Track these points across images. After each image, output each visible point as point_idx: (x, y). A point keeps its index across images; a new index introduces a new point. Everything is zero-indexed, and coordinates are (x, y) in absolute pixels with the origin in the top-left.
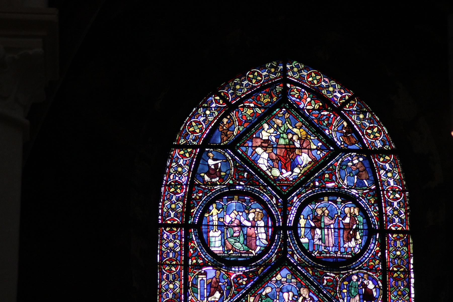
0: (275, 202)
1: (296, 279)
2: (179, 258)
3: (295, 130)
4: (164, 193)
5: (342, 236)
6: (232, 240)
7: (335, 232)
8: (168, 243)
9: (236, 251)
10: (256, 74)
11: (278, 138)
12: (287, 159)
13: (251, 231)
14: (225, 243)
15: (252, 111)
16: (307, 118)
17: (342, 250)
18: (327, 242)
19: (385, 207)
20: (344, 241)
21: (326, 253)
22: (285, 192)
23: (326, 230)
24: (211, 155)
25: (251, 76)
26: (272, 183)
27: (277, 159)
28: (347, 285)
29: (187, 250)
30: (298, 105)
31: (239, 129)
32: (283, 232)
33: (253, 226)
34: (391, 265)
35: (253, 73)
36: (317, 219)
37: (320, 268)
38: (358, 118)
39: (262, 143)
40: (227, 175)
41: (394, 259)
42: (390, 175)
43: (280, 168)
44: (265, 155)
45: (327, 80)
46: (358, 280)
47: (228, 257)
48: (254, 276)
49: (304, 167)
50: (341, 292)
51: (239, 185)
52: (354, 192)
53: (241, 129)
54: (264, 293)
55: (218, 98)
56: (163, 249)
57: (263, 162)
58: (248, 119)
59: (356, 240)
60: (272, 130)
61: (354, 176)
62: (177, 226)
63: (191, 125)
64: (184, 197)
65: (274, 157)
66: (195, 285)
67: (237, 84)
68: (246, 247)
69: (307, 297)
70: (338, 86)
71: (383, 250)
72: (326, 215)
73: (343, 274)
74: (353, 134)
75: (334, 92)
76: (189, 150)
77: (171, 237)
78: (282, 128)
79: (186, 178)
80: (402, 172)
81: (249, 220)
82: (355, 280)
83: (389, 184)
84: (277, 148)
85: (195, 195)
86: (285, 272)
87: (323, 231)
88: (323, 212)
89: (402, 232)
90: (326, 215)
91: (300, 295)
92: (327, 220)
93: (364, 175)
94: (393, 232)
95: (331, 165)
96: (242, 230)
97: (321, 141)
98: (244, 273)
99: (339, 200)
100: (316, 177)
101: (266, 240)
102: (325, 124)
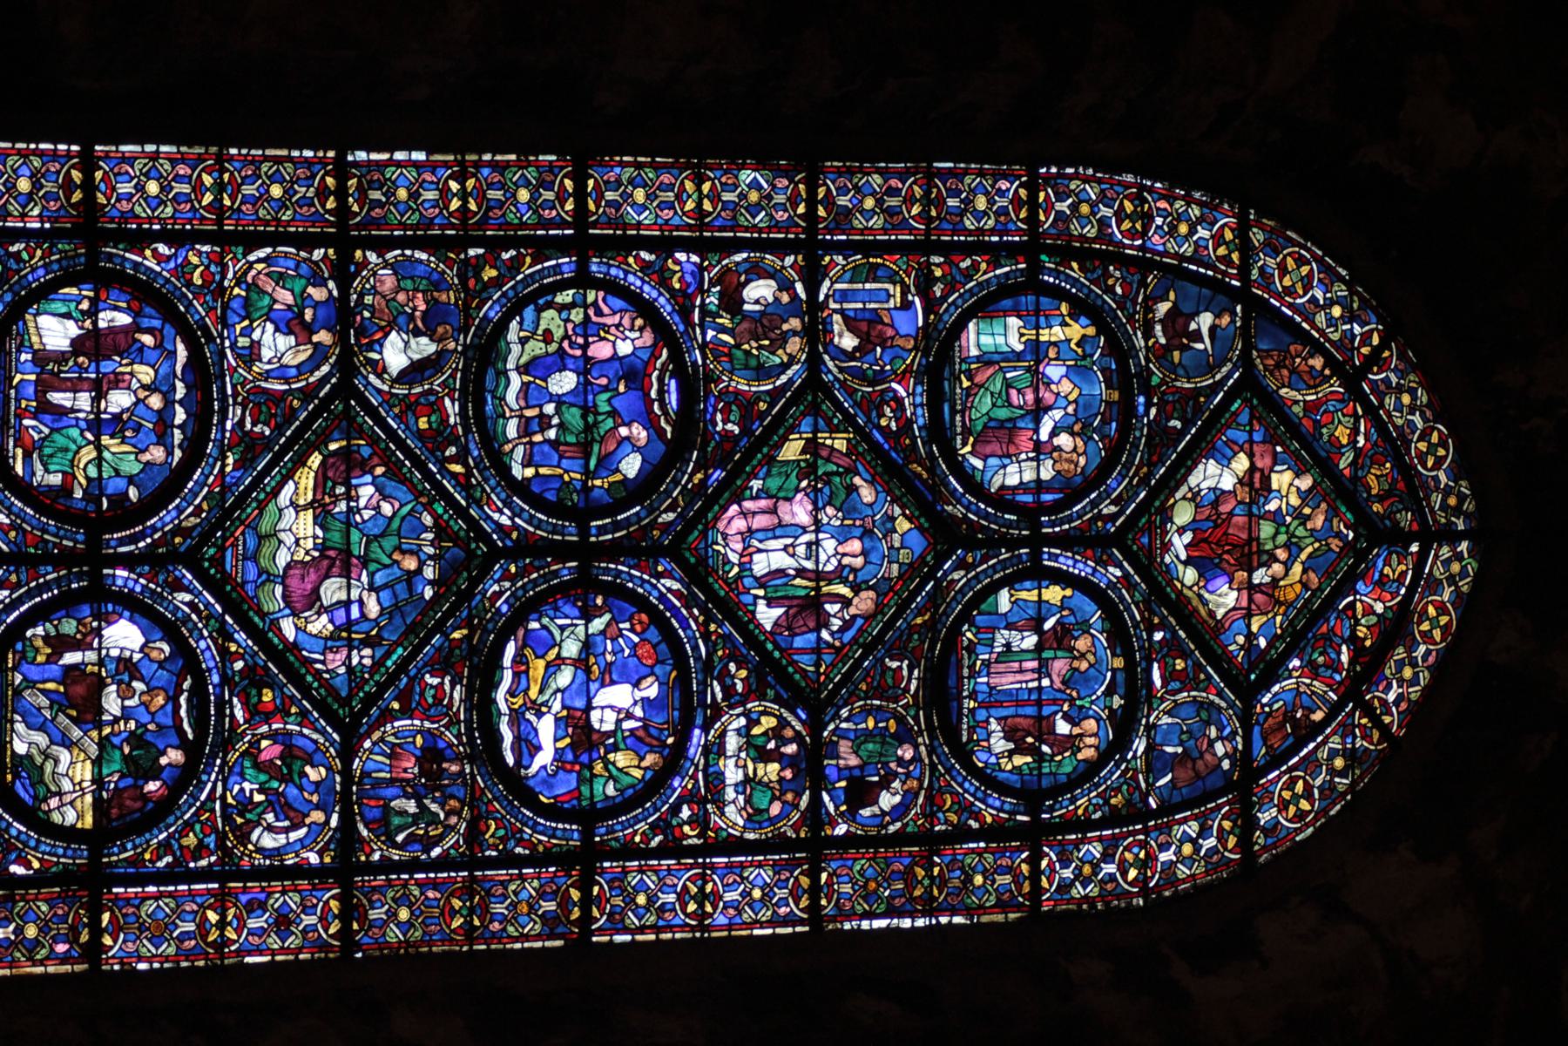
0: (1105, 511)
1: (900, 577)
2: (946, 226)
3: (1297, 569)
4: (1120, 183)
5: (1021, 711)
6: (997, 385)
7: (1030, 690)
8: (986, 193)
9: (968, 396)
10: (1441, 452)
11: (1276, 517)
12: (1225, 547)
13: (1024, 441)
14: (989, 363)
15: (1345, 441)
16: (1330, 603)
17: (981, 715)
18: (1001, 667)
19: (1100, 839)
20: (1006, 718)
21: (972, 667)
22: (1134, 540)
23: (1035, 664)
24: (1226, 320)
25: (1435, 438)
26: (1157, 503)
27: (1219, 515)
28: (886, 728)
29: (967, 249)
30: (1363, 576)
31: (1296, 402)
32: (1025, 534)
33: (1038, 447)
34: (947, 859)
35: (1443, 443)
36: (1061, 639)
37: (932, 648)
38: (1333, 754)
39: (1262, 470)
40: (1173, 368)
41: (962, 869)
42: (1188, 849)
43: (1193, 526)
44: (1228, 483)
45: (1431, 659)
46: (900, 761)
47: (952, 373)
48: (903, 450)
49: (1200, 596)
50: (867, 711)
51: (1148, 405)
52: (1140, 745)
53: (1296, 409)
54: (857, 480)
55: (1376, 340)
56: (968, 180)
57: (1213, 476)
58: (1324, 431)
59: (1011, 753)
60: (1294, 501)
61: (1181, 743)
62: (1032, 220)
63: (1301, 261)
64: (1110, 239)
65: (1225, 508)
66: (872, 273)
67: (1414, 398)
68: (979, 428)
69: (853, 610)
70: (1414, 692)
71: (985, 833)
72: (1076, 664)
73: (916, 718)
74: (1291, 740)
75: (1401, 682)
76: (1235, 257)
77: (1001, 202)
78: (1300, 532)
79: (1161, 248)
80: (1195, 887)
81: (1053, 434)
82: (900, 752)
83: (1163, 847)
84: (1250, 515)
85: (1118, 274)
86: (918, 542)
87: (1030, 656)
88: (1083, 656)
89: (1037, 890)
90: (1076, 664)
91: (856, 589)
92: (1060, 666)
93: (1185, 774)
94: (1034, 861)
95: (1209, 677)
96: (1028, 412)
97: (1270, 645)
98: (910, 422)
99: (1117, 702)
100: (1175, 633)
101: (1003, 487)
102: (1315, 655)
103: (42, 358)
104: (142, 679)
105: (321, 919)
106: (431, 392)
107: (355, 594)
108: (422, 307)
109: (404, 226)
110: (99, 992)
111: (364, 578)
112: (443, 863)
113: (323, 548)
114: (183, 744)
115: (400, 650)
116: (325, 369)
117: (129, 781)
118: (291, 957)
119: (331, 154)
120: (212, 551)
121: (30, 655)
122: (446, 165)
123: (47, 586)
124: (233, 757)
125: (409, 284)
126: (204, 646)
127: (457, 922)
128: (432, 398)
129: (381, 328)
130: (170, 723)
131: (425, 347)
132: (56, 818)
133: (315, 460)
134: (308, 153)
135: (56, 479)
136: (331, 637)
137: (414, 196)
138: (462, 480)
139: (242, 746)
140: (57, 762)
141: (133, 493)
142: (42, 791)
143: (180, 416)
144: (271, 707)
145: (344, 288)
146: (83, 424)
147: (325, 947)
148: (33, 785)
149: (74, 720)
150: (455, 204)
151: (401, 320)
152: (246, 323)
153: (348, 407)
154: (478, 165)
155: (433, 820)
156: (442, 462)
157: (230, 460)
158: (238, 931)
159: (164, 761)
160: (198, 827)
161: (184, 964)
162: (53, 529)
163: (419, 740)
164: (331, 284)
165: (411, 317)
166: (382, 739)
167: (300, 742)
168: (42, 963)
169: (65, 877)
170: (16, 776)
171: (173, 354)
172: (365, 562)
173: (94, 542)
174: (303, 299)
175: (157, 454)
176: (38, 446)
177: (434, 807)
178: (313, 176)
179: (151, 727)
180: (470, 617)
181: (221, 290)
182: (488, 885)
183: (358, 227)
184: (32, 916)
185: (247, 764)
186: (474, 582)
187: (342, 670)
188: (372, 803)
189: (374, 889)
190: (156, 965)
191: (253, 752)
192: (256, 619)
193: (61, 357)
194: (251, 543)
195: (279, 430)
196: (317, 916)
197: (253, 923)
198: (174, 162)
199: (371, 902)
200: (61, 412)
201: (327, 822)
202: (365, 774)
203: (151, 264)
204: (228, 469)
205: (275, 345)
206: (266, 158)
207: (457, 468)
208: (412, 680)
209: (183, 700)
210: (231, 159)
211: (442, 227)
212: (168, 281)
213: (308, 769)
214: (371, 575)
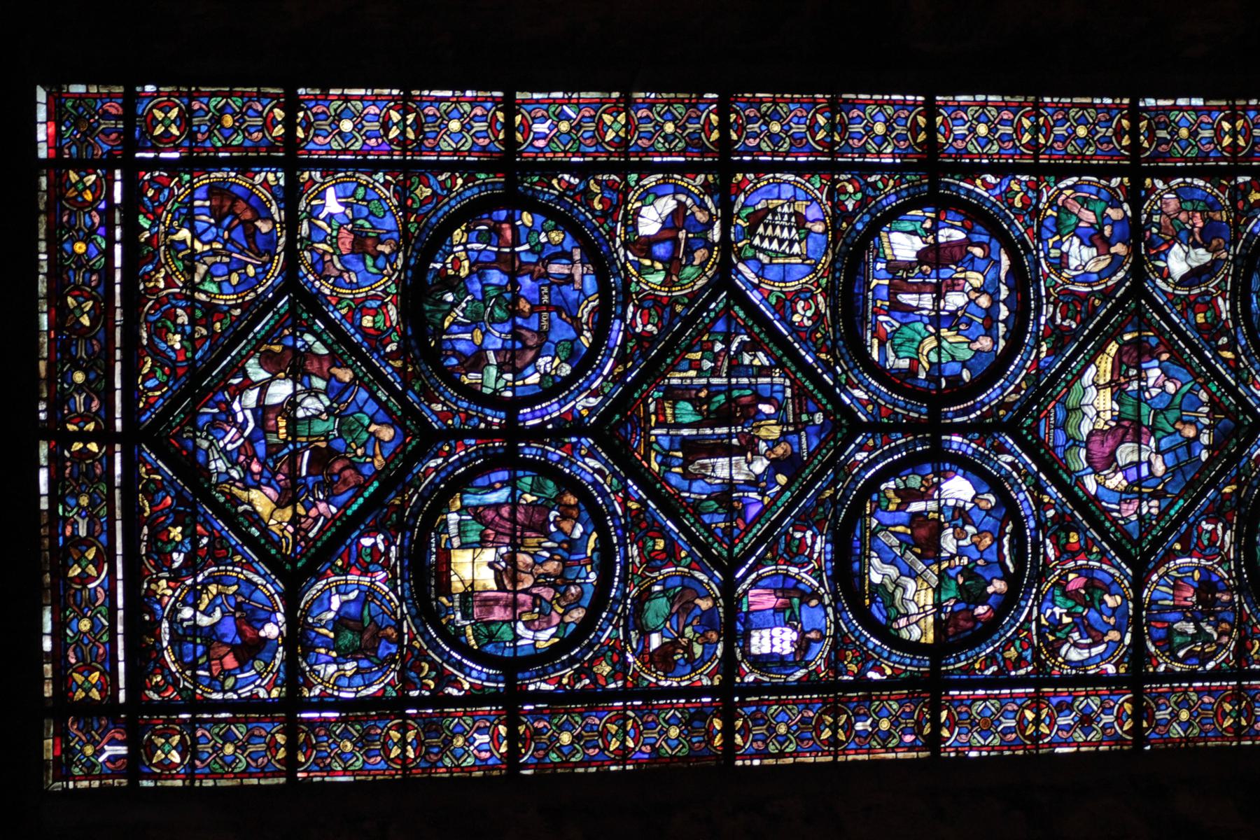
103: (894, 267)
104: (973, 524)
105: (1117, 718)
106: (1207, 293)
107: (1144, 456)
108: (1200, 224)
109: (1184, 159)
110: (938, 775)
111: (1152, 443)
112: (1216, 674)
113: (1119, 419)
114: (1006, 576)
115: (1181, 502)
116: (1121, 274)
117: (962, 606)
118: (1093, 749)
119: (1126, 101)
120: (1029, 421)
121: (884, 504)
122: (1220, 109)
123: (898, 449)
124: (1046, 587)
125: (1189, 205)
126: (1023, 497)
127: (1228, 723)
128: (1208, 298)
129: (1166, 242)
130: (995, 558)
131: (1202, 256)
132: (904, 634)
133: (1113, 348)
134: (1108, 101)
135: (904, 364)
136: (1126, 491)
137: (1193, 134)
138: (1232, 364)
139: (1053, 578)
140: (905, 590)
141: (966, 375)
142: (893, 613)
143: (1004, 312)
144: (1077, 547)
145: (1136, 209)
146: (926, 320)
147: (1119, 740)
148: (886, 608)
149: (919, 557)
150: (1227, 141)
151: (1183, 235)
152: (1057, 238)
153: (1139, 305)
154: (1246, 108)
155: (1208, 639)
156: (1216, 350)
157: (1044, 348)
158: (1050, 726)
159: (990, 590)
160: (1018, 643)
161: (1007, 753)
162: (902, 404)
163: (1197, 575)
164: (1126, 206)
165: (1191, 233)
166: (1166, 574)
167: (1100, 575)
168: (893, 750)
169: (912, 682)
170: (873, 601)
171: (999, 262)
172: (1153, 430)
173: (935, 414)
174: (1103, 218)
175: (985, 343)
176: (891, 336)
177: (1209, 629)
178: (1112, 119)
179: (980, 562)
180: (1239, 475)
181: (1037, 212)
182: (1252, 693)
183: (1148, 160)
184: (885, 713)
185: (1057, 592)
186: (1242, 447)
187: (1134, 518)
188: (1159, 625)
189: (1160, 695)
190: (984, 753)
191: (1062, 583)
192: (1065, 476)
193: (909, 266)
194: (1061, 415)
195: (1083, 324)
196: (1114, 717)
197: (1062, 721)
198: (999, 108)
199: (1158, 705)
200: (908, 309)
201: (1122, 640)
202: (1153, 602)
203: (981, 191)
204: (1043, 355)
205: (1080, 255)
206: (1074, 105)
207: (1228, 355)
208: (1190, 526)
209: (1006, 541)
210: (1045, 105)
211: (1216, 159)
212: (994, 204)
213: (1106, 597)
214: (1158, 441)
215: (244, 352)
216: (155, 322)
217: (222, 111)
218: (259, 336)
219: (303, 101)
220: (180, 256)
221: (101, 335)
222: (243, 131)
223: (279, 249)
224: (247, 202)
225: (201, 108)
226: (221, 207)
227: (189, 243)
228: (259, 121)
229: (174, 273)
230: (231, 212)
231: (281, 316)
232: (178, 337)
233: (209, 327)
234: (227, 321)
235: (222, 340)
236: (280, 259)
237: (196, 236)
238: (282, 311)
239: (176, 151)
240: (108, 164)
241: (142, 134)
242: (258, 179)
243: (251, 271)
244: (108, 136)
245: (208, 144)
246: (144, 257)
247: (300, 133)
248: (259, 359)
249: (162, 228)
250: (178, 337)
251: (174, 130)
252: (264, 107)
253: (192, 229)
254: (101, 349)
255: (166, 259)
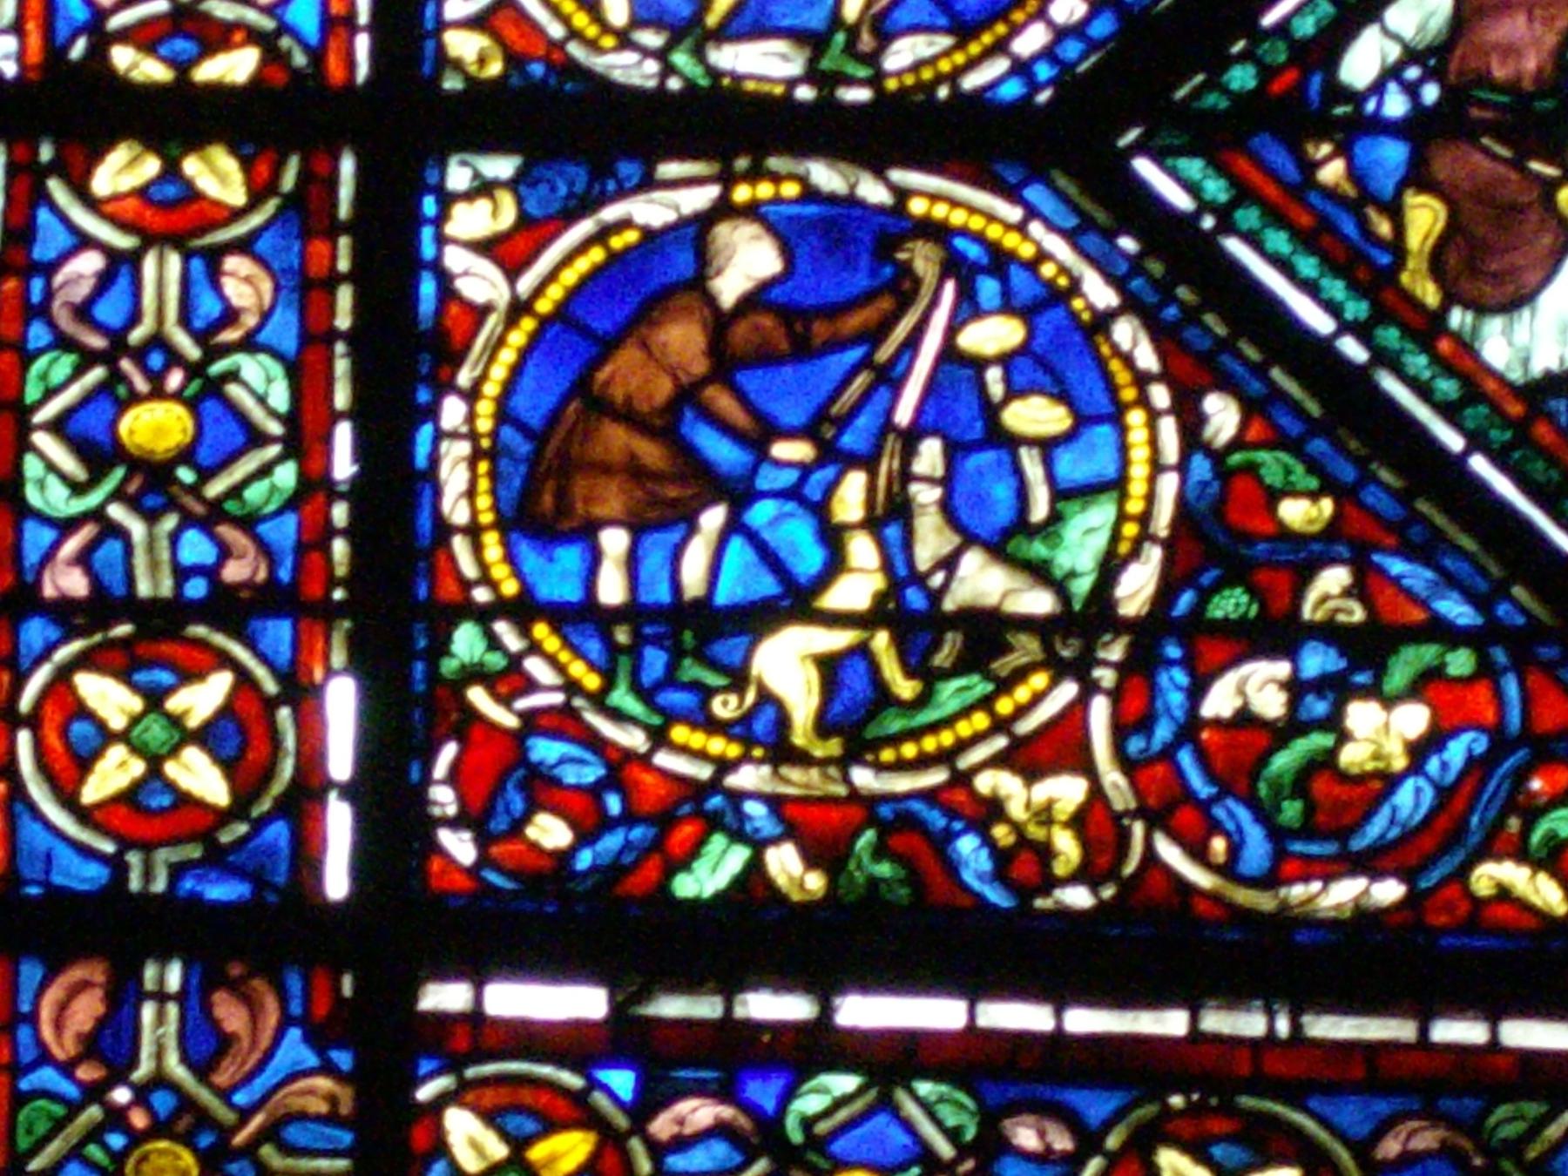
215: (1447, 387)
216: (1278, 836)
217: (100, 453)
218: (1357, 309)
219: (55, 51)
220: (906, 689)
221: (1353, 1114)
222: (214, 352)
223: (873, 192)
224: (607, 346)
225: (84, 559)
226: (635, 471)
227: (841, 639)
228: (163, 273)
229: (1001, 725)
230: (665, 425)
231: (1243, 194)
232: (1362, 716)
233: (1304, 556)
234: (1273, 465)
235: (1371, 496)
236: (931, 192)
237: (796, 601)
238: (1216, 189)
239: (317, 691)
240: (387, 1053)
241: (218, 860)
242: (481, 282)
243: (993, 335)
244: (224, 1042)
245: (283, 532)
246: (914, 878)
247: (235, 66)
248: (1482, 309)
249: (749, 777)
250: (1362, 716)
251: (201, 699)
252: (84, 242)
253: (757, 619)
254: (1432, 1115)
255: (924, 762)
